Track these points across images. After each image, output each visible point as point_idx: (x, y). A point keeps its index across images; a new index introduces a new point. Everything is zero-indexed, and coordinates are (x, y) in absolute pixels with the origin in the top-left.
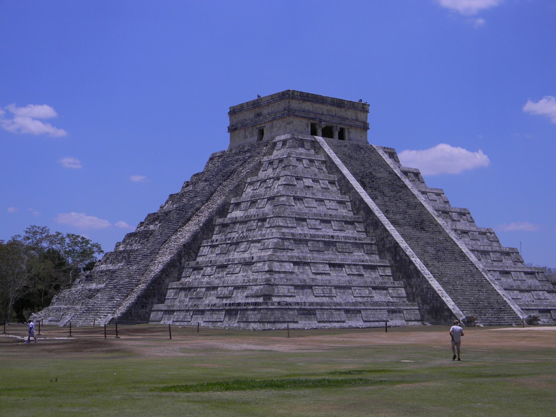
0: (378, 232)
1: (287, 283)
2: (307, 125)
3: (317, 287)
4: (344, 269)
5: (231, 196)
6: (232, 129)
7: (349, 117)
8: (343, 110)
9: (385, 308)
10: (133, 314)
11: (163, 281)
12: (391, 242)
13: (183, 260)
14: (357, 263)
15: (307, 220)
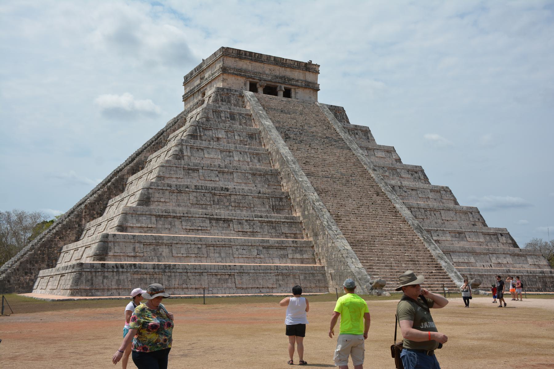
0: (290, 184)
1: (132, 241)
2: (245, 84)
3: (179, 246)
4: (231, 225)
5: (149, 154)
6: (186, 98)
7: (297, 78)
8: (288, 69)
9: (272, 271)
10: (12, 281)
11: (56, 244)
12: (300, 196)
13: (83, 222)
14: (251, 219)
15: (200, 171)
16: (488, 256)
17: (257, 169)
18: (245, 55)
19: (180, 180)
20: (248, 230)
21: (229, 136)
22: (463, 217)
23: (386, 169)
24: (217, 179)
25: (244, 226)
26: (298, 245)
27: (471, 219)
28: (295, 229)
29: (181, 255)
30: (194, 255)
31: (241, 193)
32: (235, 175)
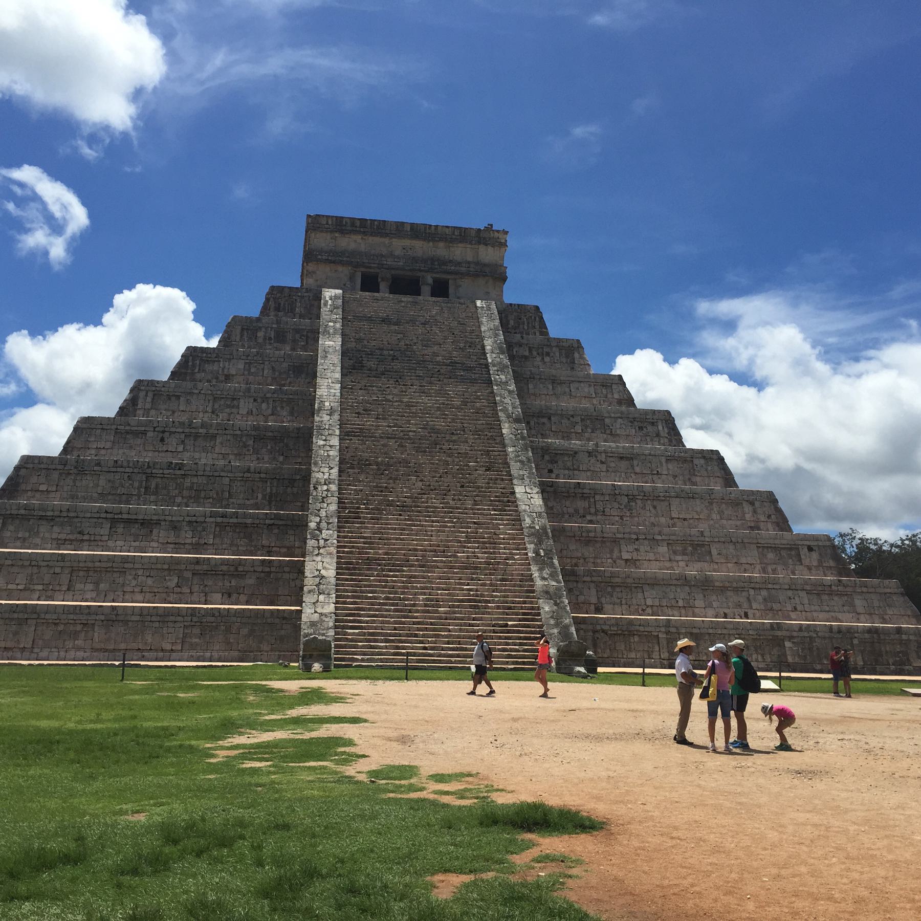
2: (352, 278)
3: (15, 570)
4: (155, 531)
8: (441, 244)
16: (744, 594)
17: (267, 428)
18: (353, 225)
19: (103, 452)
20: (189, 541)
21: (253, 370)
22: (728, 512)
23: (578, 419)
24: (180, 448)
25: (183, 534)
26: (273, 569)
27: (748, 516)
28: (292, 538)
29: (14, 587)
30: (40, 587)
31: (207, 473)
32: (219, 440)
